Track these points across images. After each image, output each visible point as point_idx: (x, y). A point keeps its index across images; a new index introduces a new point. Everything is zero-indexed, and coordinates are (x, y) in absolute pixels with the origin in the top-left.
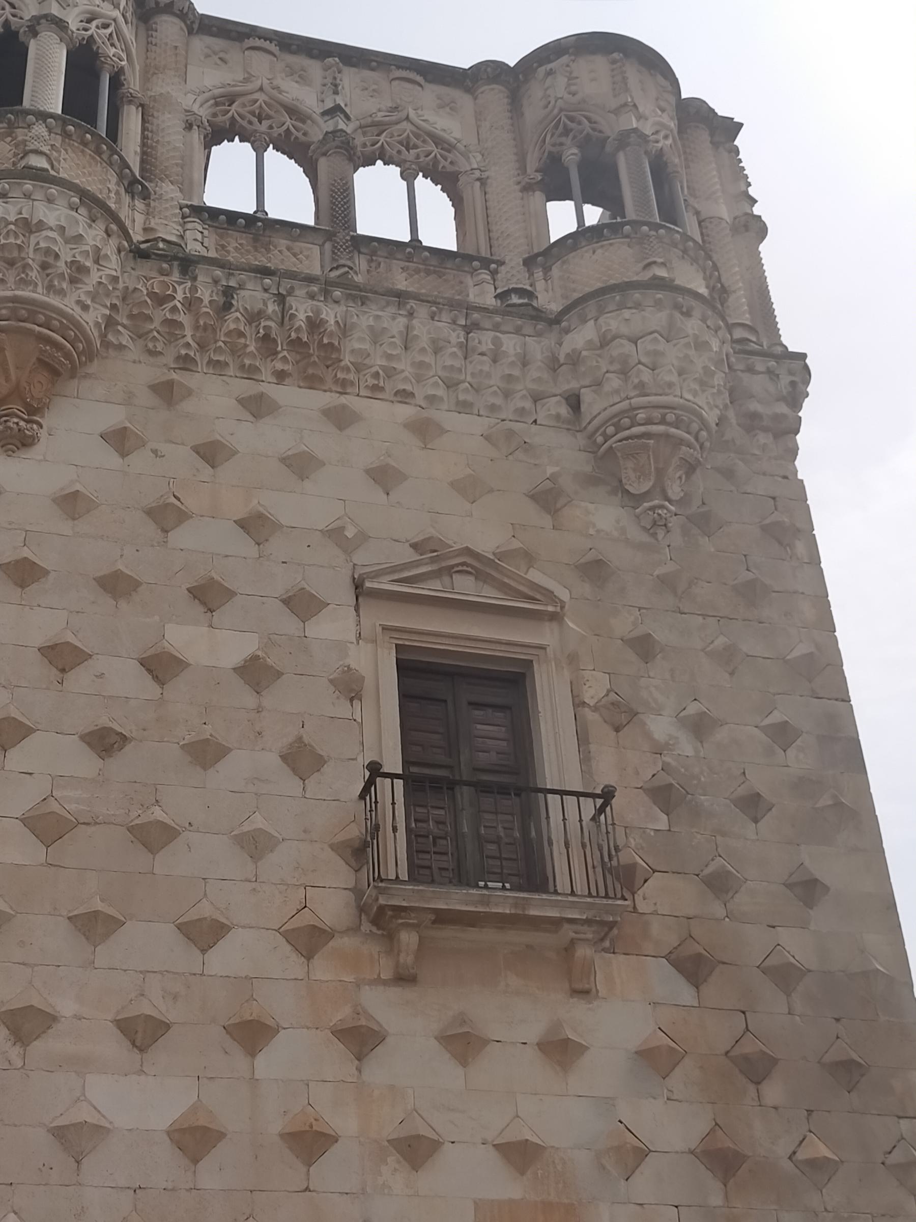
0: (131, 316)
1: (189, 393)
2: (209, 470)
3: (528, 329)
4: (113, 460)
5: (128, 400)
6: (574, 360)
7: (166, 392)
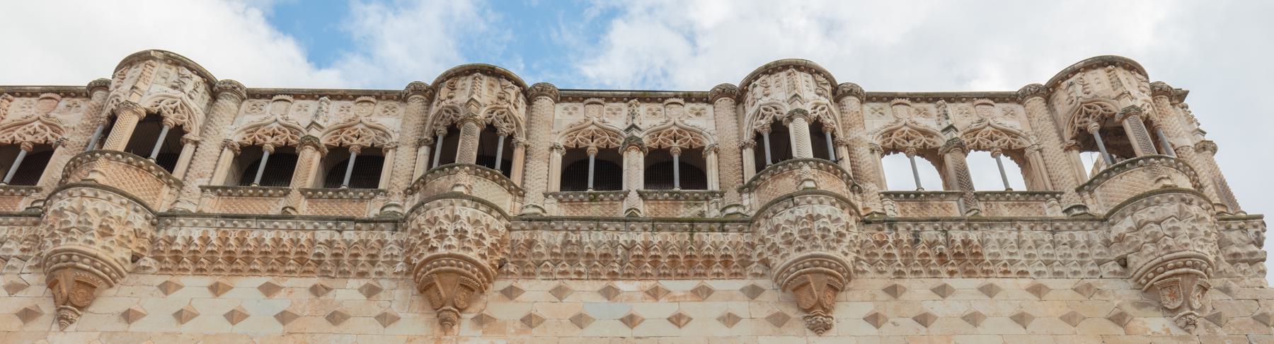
0: (867, 255)
1: (905, 289)
2: (923, 329)
3: (1089, 227)
4: (872, 330)
5: (873, 298)
6: (1120, 239)
7: (893, 291)
